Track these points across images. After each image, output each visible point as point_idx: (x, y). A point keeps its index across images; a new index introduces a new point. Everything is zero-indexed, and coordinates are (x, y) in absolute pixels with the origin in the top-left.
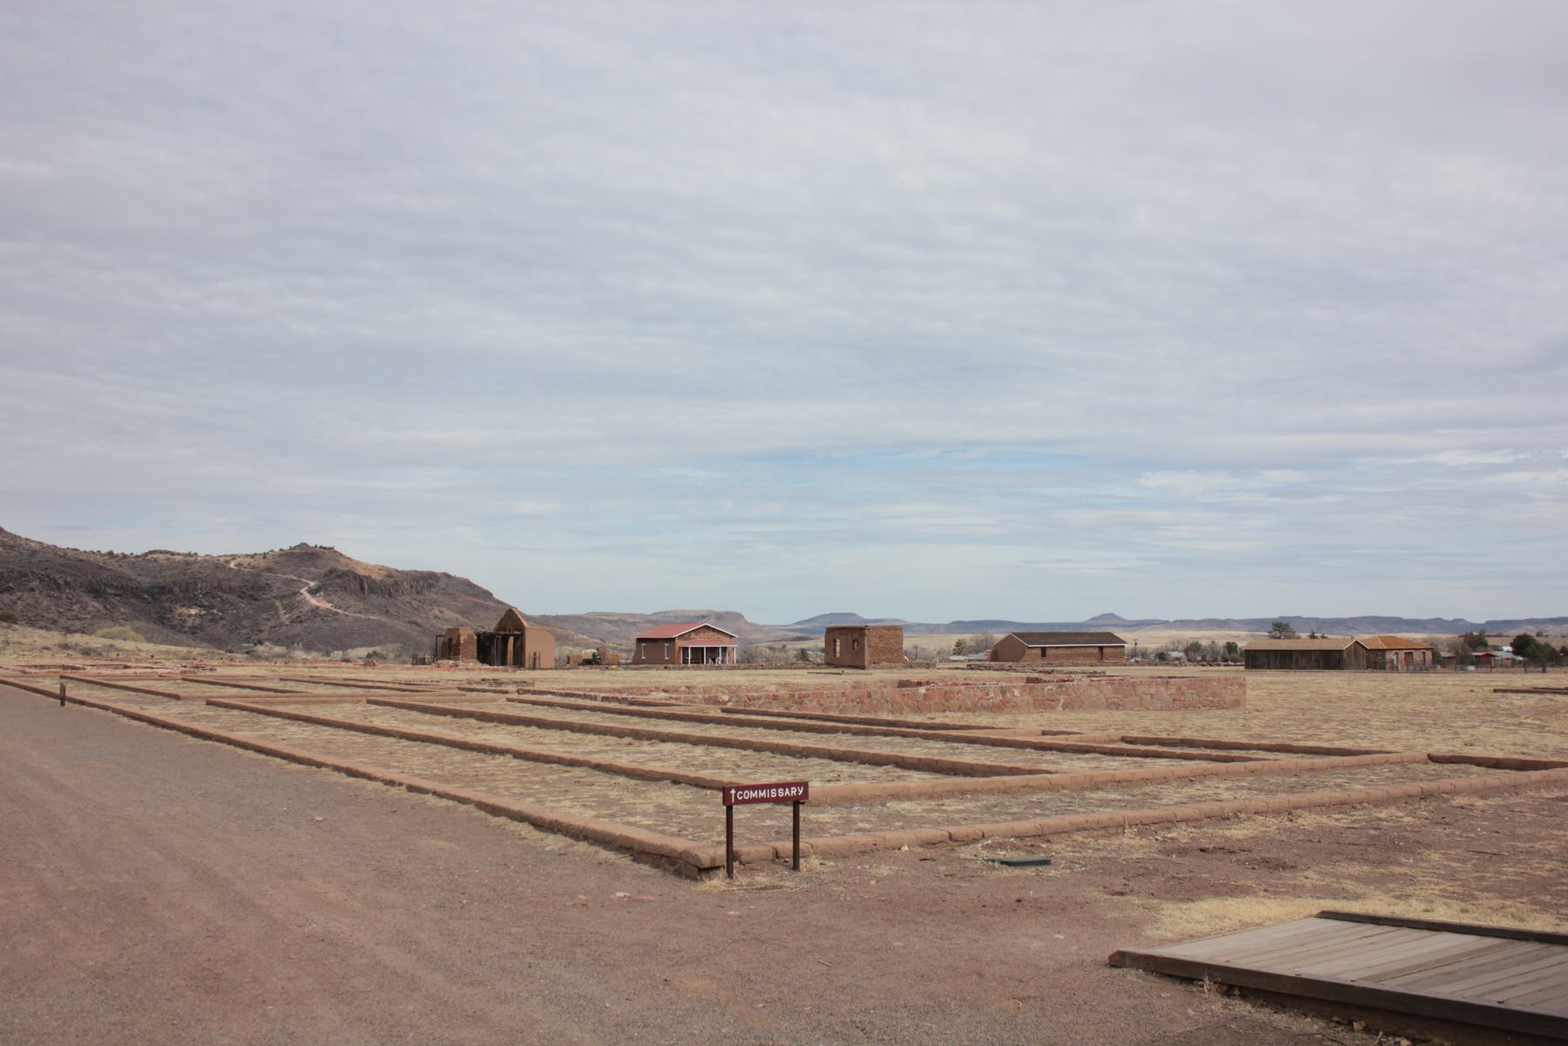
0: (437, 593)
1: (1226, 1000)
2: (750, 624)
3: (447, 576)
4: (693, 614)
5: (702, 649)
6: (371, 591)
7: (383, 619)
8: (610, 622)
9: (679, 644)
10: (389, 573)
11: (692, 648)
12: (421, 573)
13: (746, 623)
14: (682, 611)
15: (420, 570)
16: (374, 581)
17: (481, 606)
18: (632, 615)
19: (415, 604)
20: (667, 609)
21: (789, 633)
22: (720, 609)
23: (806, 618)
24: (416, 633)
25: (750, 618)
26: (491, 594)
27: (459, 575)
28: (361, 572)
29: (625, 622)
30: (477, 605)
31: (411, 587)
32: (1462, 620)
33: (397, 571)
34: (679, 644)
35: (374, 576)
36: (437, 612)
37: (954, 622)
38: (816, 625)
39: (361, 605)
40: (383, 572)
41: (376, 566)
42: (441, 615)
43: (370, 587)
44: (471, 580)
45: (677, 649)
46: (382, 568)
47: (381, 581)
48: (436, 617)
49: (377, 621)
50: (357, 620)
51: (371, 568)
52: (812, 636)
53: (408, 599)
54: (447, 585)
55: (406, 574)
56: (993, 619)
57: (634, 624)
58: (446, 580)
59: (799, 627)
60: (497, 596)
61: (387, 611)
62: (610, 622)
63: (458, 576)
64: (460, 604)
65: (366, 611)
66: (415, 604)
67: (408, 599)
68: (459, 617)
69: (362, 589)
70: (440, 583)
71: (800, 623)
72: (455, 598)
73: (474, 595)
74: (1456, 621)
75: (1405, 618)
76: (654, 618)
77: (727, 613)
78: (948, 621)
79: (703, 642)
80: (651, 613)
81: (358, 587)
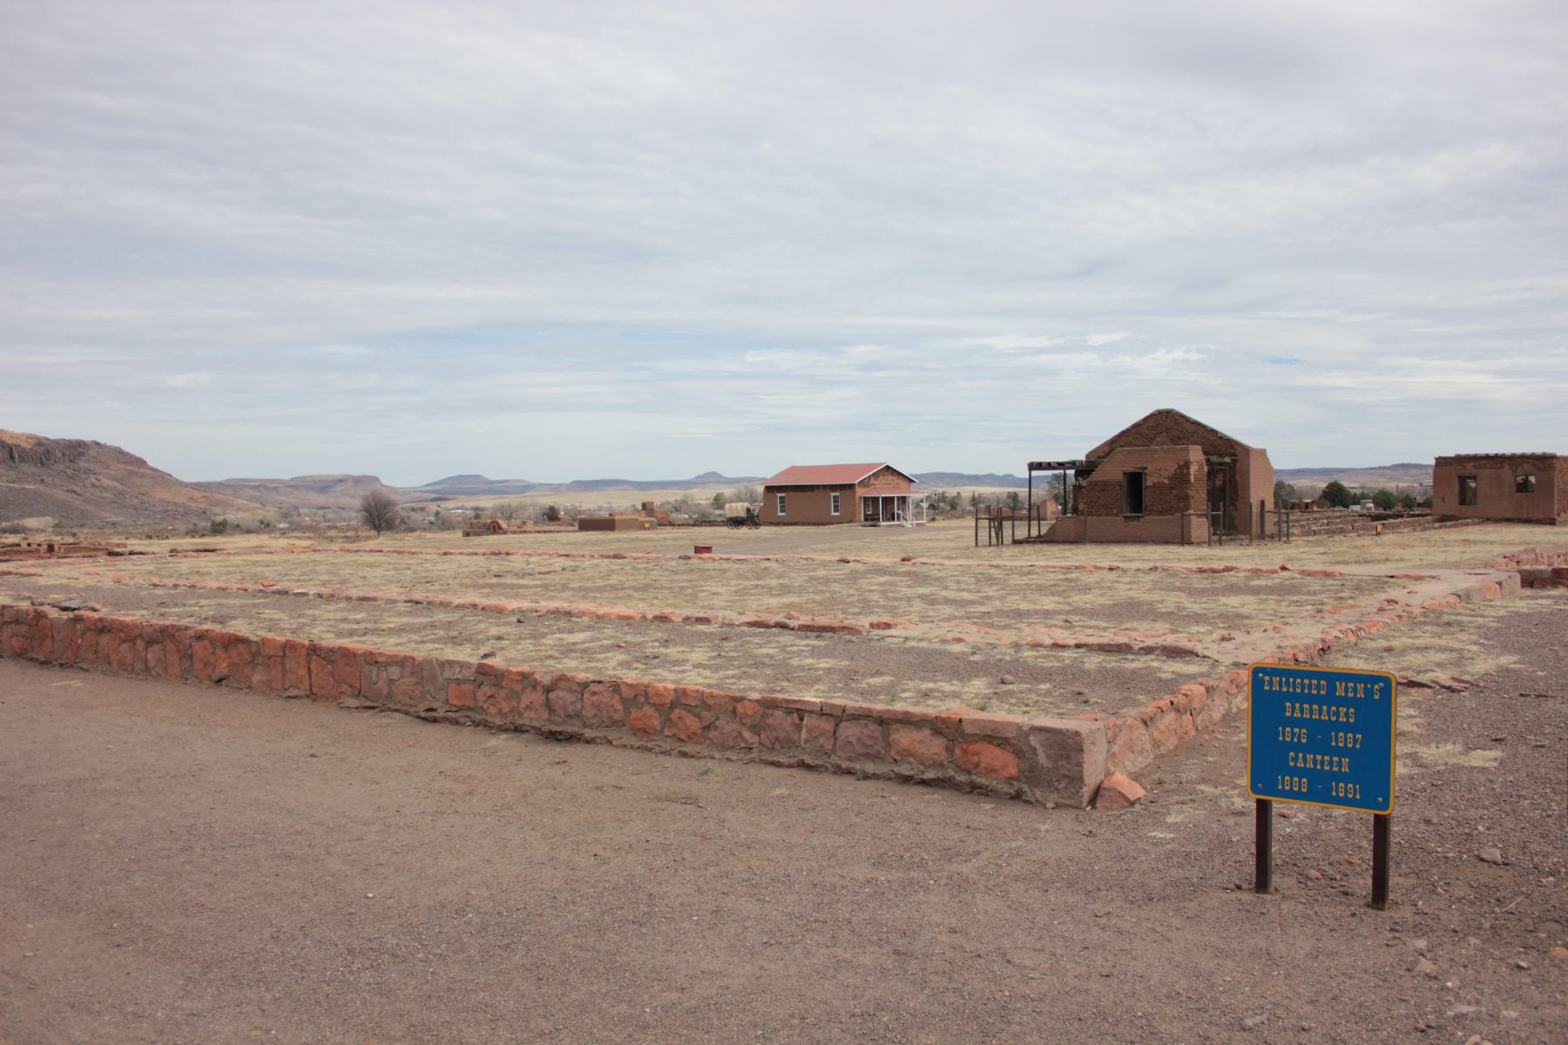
0: (88, 461)
1: (1086, 746)
2: (386, 487)
3: (98, 444)
4: (330, 479)
5: (893, 498)
6: (22, 460)
7: (41, 488)
8: (251, 488)
9: (861, 492)
10: (40, 442)
11: (883, 498)
12: (69, 441)
13: (383, 485)
14: (320, 476)
15: (67, 438)
16: (24, 449)
17: (136, 473)
18: (272, 481)
19: (69, 472)
20: (306, 474)
21: (424, 495)
22: (356, 472)
23: (435, 480)
24: (78, 502)
25: (385, 481)
26: (145, 462)
27: (109, 443)
28: (9, 441)
29: (267, 488)
30: (131, 473)
31: (64, 455)
32: (1011, 475)
33: (47, 439)
34: (861, 492)
35: (23, 445)
36: (93, 480)
37: (574, 482)
38: (445, 486)
39: (13, 474)
40: (32, 441)
41: (23, 434)
42: (97, 483)
43: (20, 456)
44: (122, 448)
45: (857, 500)
46: (30, 437)
47: (31, 449)
48: (93, 485)
49: (35, 492)
50: (11, 490)
51: (19, 436)
52: (450, 496)
53: (61, 467)
54: (98, 453)
55: (56, 442)
56: (1492, 451)
57: (275, 489)
58: (97, 449)
59: (428, 488)
60: (151, 463)
61: (42, 480)
62: (251, 488)
63: (109, 444)
64: (113, 472)
65: (20, 480)
66: (69, 472)
67: (61, 467)
68: (117, 484)
69: (12, 457)
70: (90, 452)
71: (429, 485)
72: (108, 467)
73: (125, 463)
74: (1006, 476)
75: (966, 473)
76: (293, 483)
77: (364, 477)
78: (568, 480)
79: (882, 490)
80: (289, 478)
81: (7, 456)
